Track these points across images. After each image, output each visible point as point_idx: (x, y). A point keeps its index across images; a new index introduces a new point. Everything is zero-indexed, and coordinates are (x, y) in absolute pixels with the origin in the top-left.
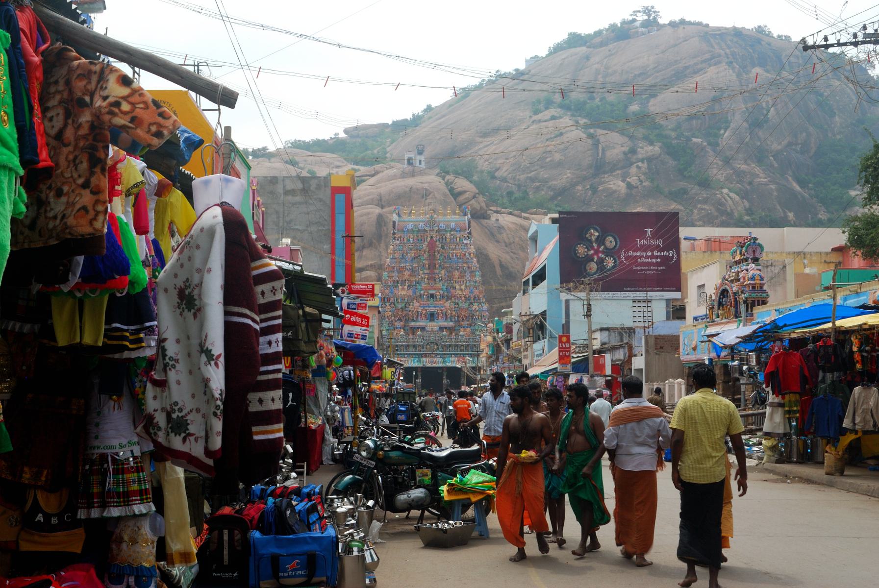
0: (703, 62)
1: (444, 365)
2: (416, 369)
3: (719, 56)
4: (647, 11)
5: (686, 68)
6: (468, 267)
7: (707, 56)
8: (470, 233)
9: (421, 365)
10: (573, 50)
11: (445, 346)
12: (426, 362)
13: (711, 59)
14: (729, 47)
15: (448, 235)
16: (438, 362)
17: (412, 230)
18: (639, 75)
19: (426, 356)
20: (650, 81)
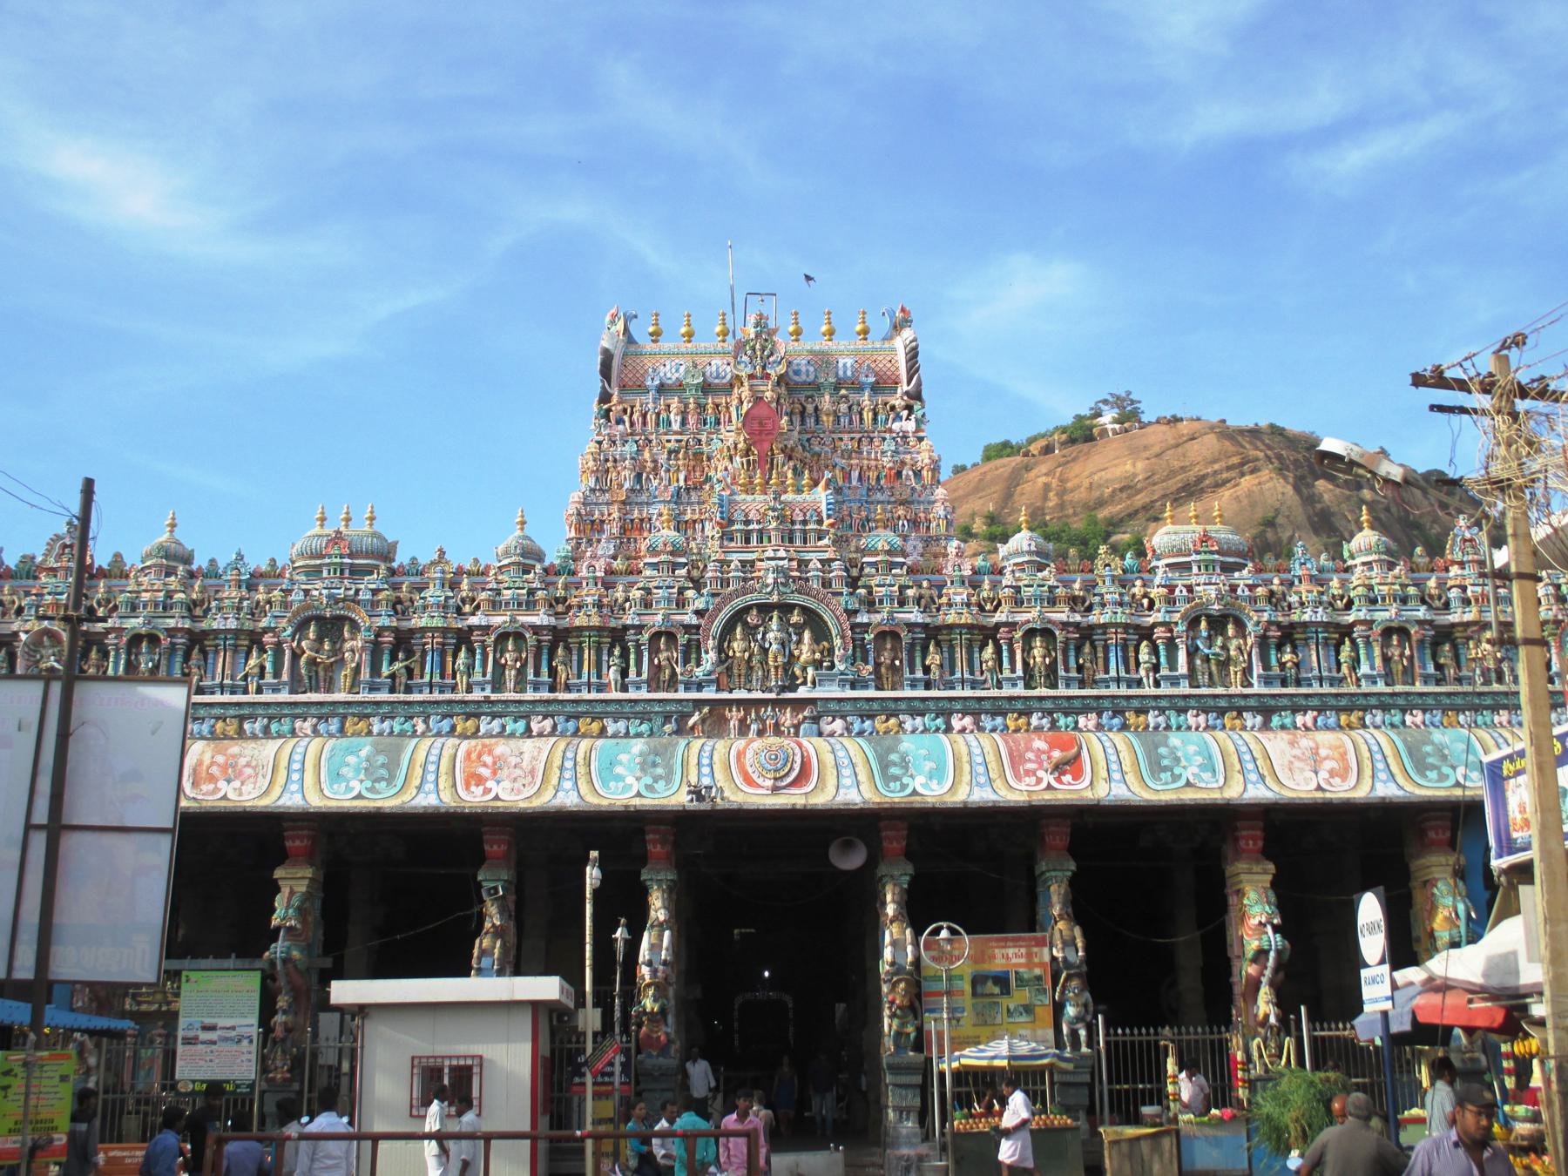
0: (1229, 468)
1: (894, 796)
2: (620, 835)
3: (1257, 459)
4: (1118, 402)
5: (1204, 477)
6: (915, 523)
7: (1236, 460)
8: (916, 395)
9: (679, 798)
10: (999, 462)
11: (888, 635)
12: (735, 772)
13: (1242, 464)
14: (1269, 447)
15: (826, 402)
16: (842, 773)
17: (680, 387)
18: (1121, 490)
19: (715, 719)
20: (1140, 500)
